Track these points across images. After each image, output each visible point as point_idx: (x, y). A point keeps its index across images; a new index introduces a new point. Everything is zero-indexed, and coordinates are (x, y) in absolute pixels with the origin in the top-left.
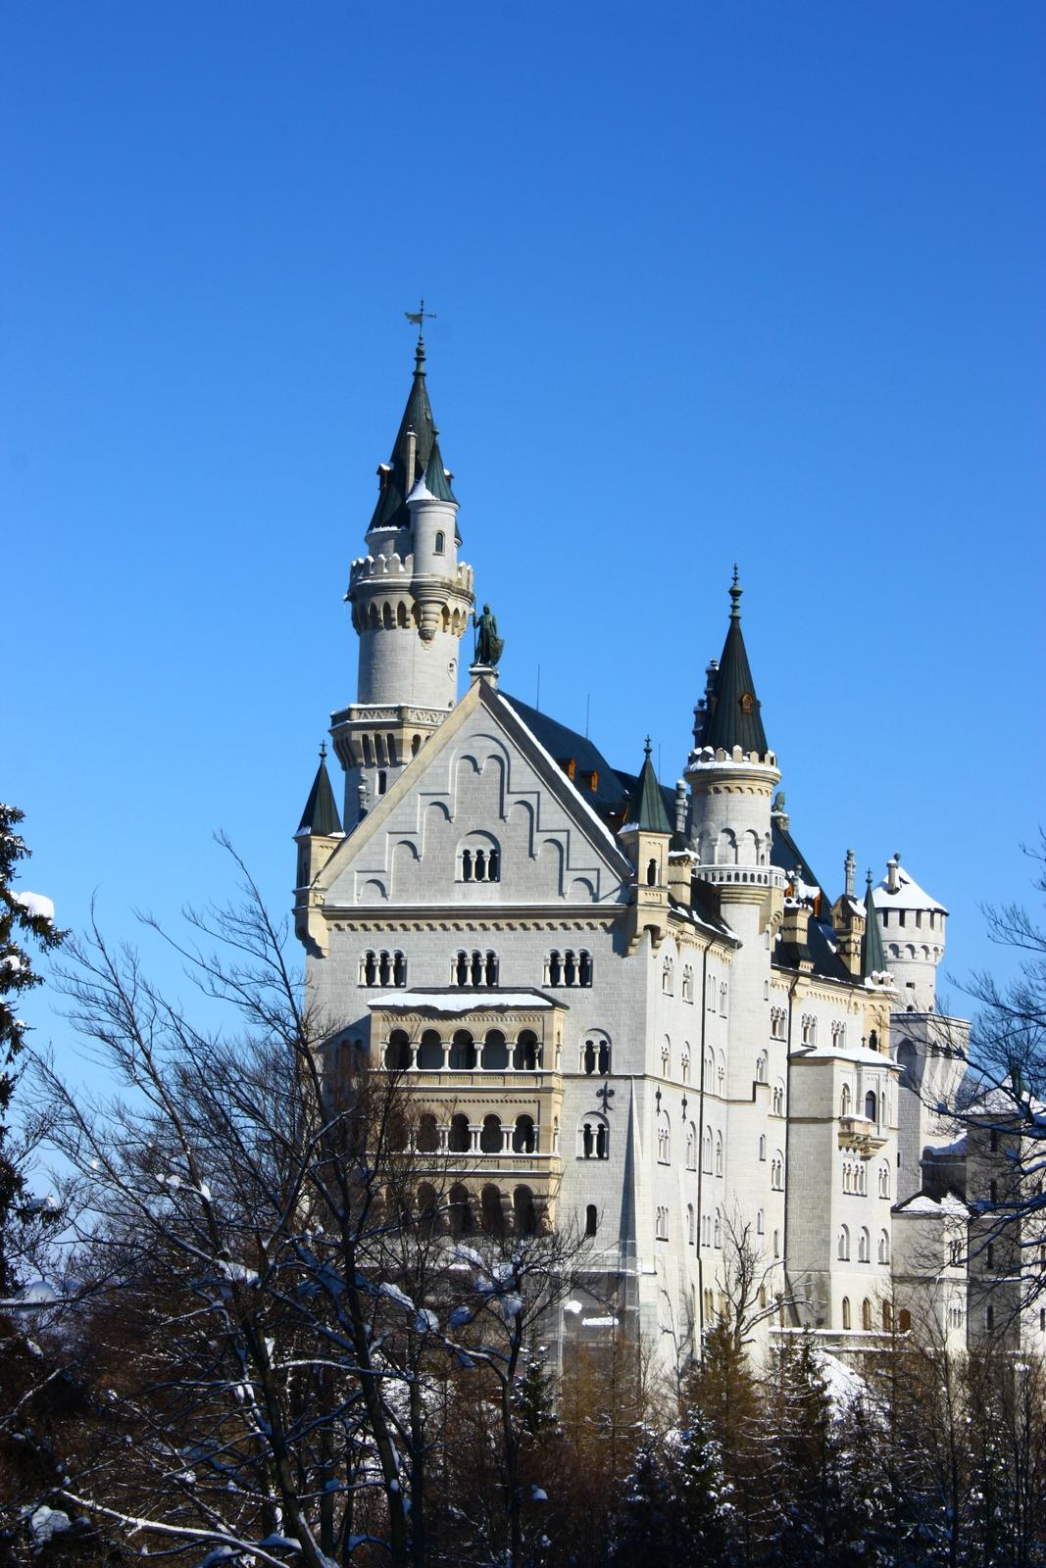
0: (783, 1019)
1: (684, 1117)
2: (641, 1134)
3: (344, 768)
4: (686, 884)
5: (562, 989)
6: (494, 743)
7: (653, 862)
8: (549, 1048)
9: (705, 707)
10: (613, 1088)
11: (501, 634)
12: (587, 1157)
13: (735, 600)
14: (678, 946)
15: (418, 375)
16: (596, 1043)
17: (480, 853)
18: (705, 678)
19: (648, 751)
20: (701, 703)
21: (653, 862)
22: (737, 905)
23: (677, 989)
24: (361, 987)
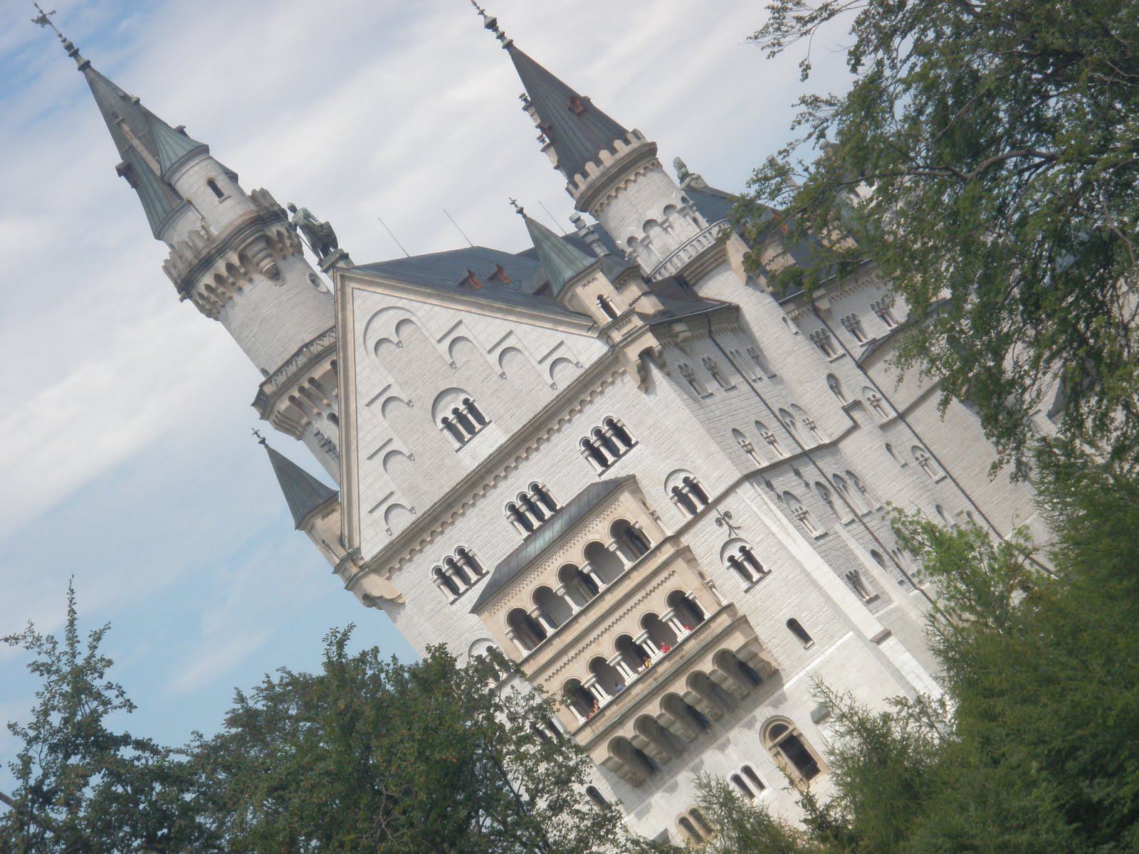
1: (807, 485)
3: (299, 438)
5: (616, 465)
6: (391, 312)
7: (600, 297)
9: (547, 141)
10: (726, 510)
11: (321, 218)
13: (496, 30)
14: (682, 349)
16: (681, 485)
17: (456, 411)
18: (526, 114)
19: (521, 211)
20: (541, 139)
21: (600, 297)
24: (452, 603)
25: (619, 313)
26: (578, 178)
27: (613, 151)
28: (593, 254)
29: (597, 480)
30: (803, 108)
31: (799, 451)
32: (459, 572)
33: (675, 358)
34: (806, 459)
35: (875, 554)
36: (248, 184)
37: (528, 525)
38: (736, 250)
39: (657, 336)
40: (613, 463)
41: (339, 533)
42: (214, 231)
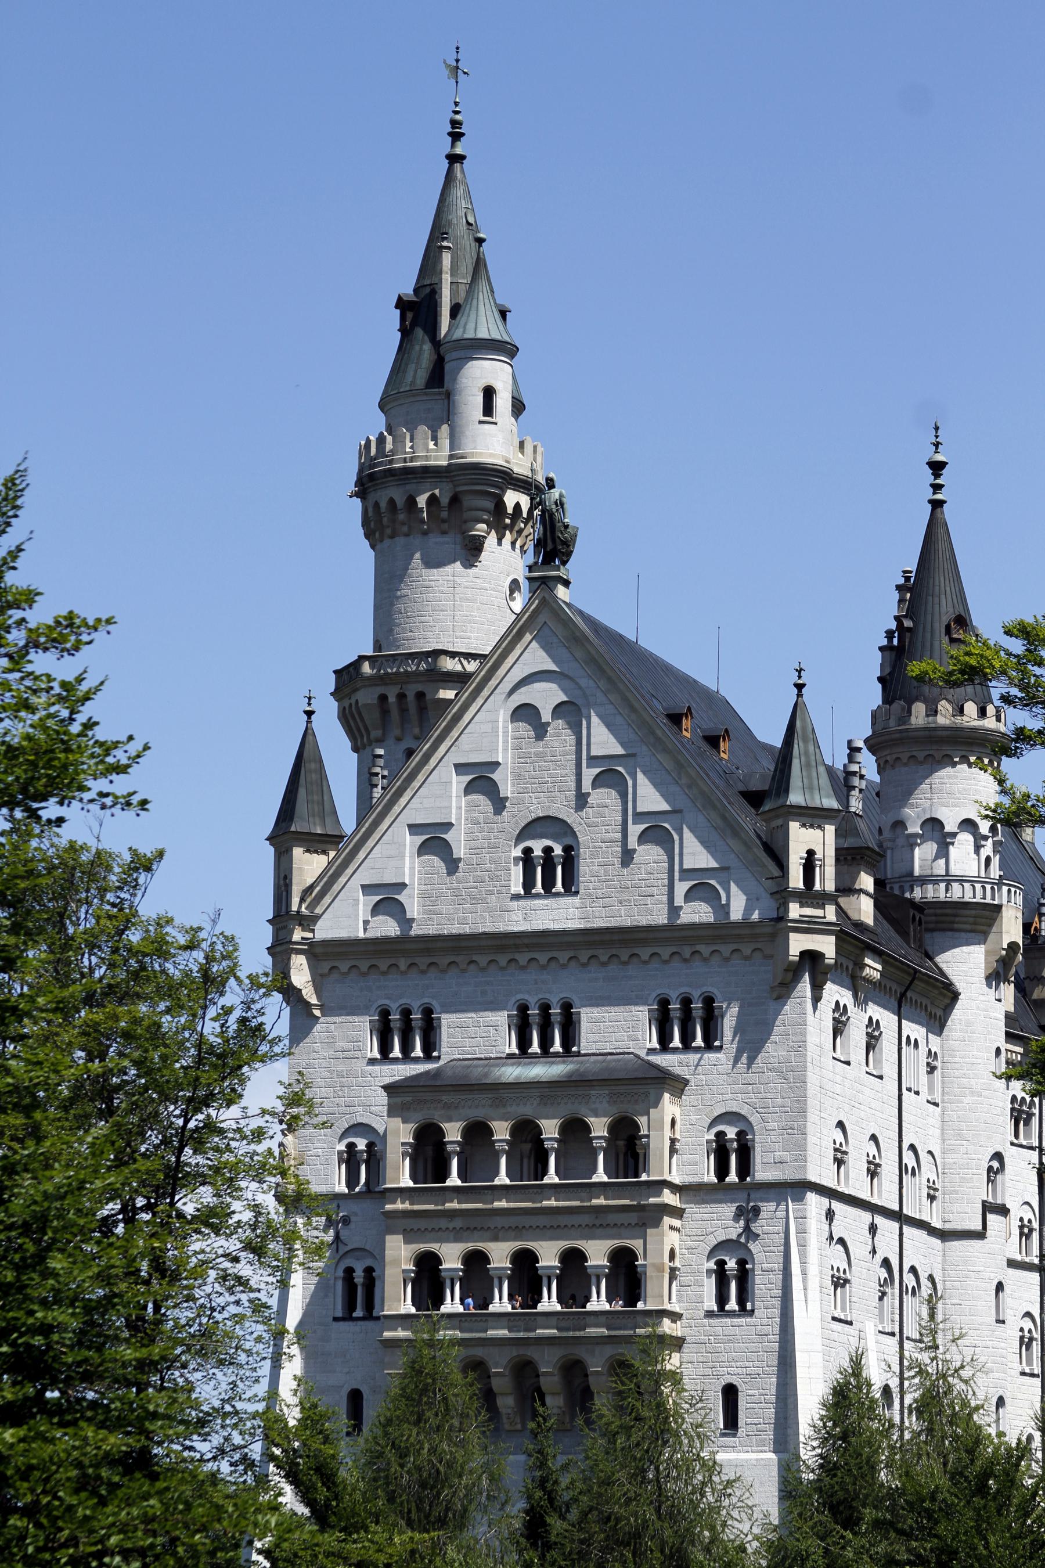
0: (1030, 1115)
1: (874, 1251)
2: (804, 1273)
3: (355, 749)
4: (867, 894)
7: (811, 853)
9: (895, 642)
13: (937, 475)
15: (454, 159)
17: (548, 850)
18: (896, 596)
19: (800, 687)
20: (890, 634)
21: (811, 853)
22: (950, 933)
23: (858, 1054)
25: (817, 887)
28: (845, 802)
29: (642, 1053)
31: (896, 1208)
41: (310, 881)
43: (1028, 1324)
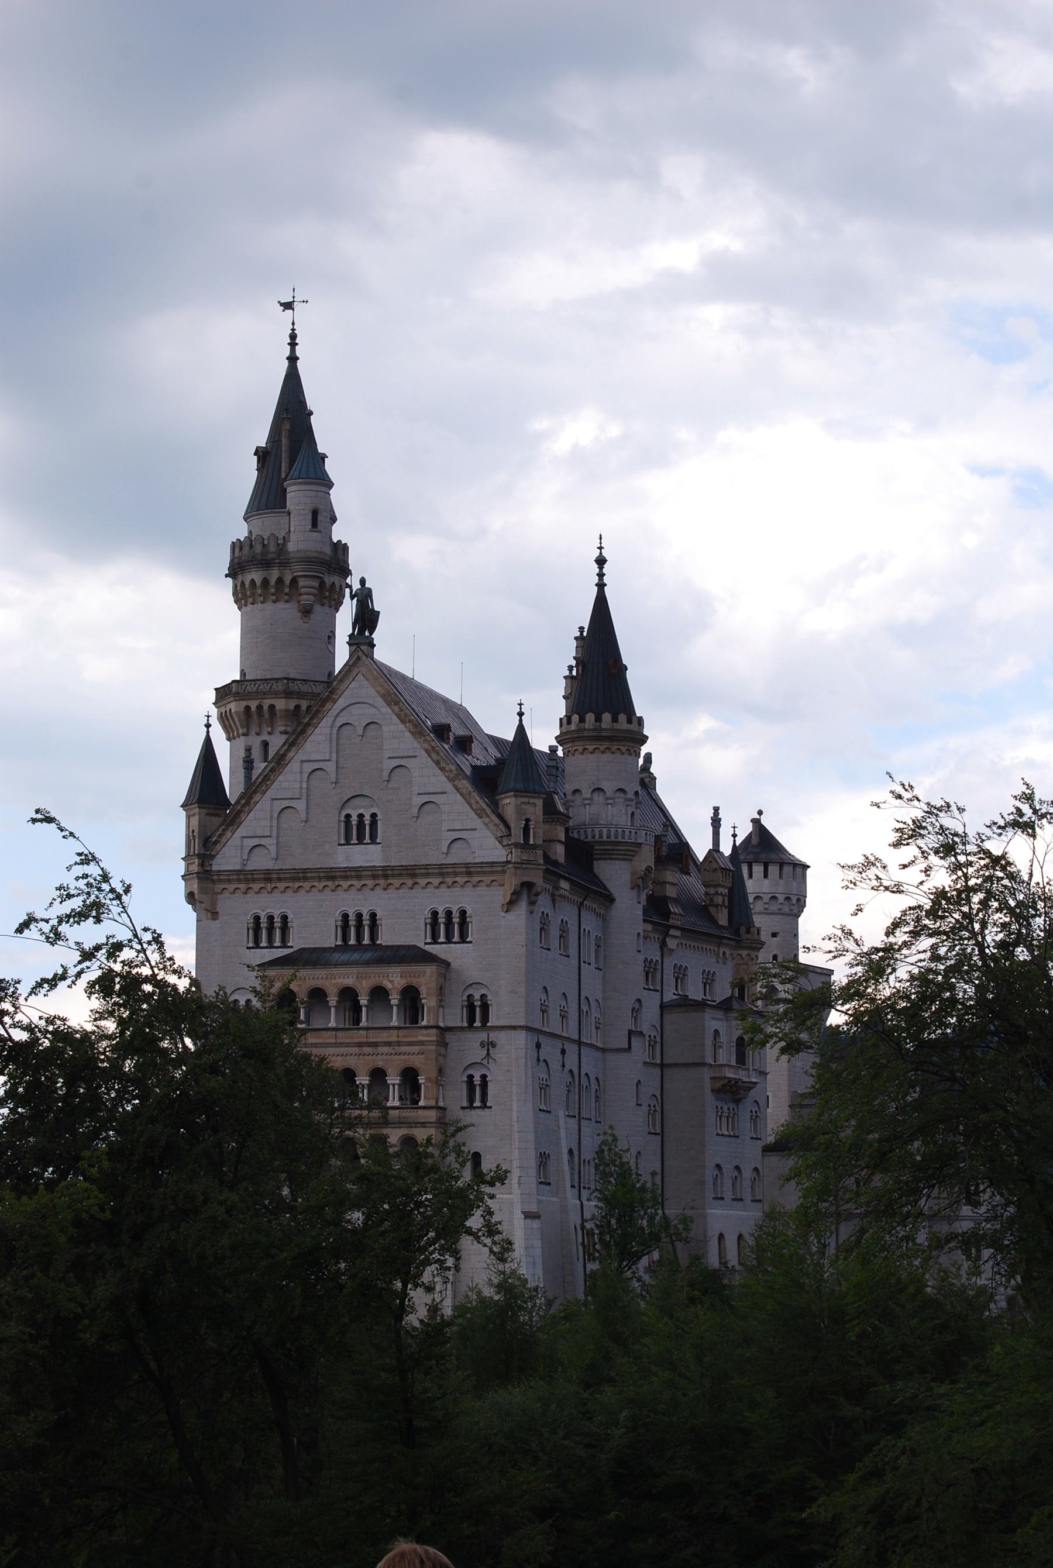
0: (655, 969)
1: (563, 1066)
3: (229, 739)
4: (560, 842)
6: (372, 711)
8: (428, 1001)
9: (574, 673)
12: (471, 1107)
13: (601, 568)
14: (554, 901)
15: (293, 359)
16: (477, 996)
17: (361, 816)
18: (574, 643)
19: (521, 714)
20: (570, 668)
23: (554, 943)
25: (531, 842)
26: (575, 718)
27: (615, 720)
29: (421, 945)
30: (839, 933)
32: (271, 929)
33: (544, 903)
34: (576, 1047)
35: (571, 1152)
36: (338, 533)
37: (345, 937)
38: (646, 859)
39: (544, 878)
40: (442, 943)
42: (291, 547)
43: (653, 1102)
